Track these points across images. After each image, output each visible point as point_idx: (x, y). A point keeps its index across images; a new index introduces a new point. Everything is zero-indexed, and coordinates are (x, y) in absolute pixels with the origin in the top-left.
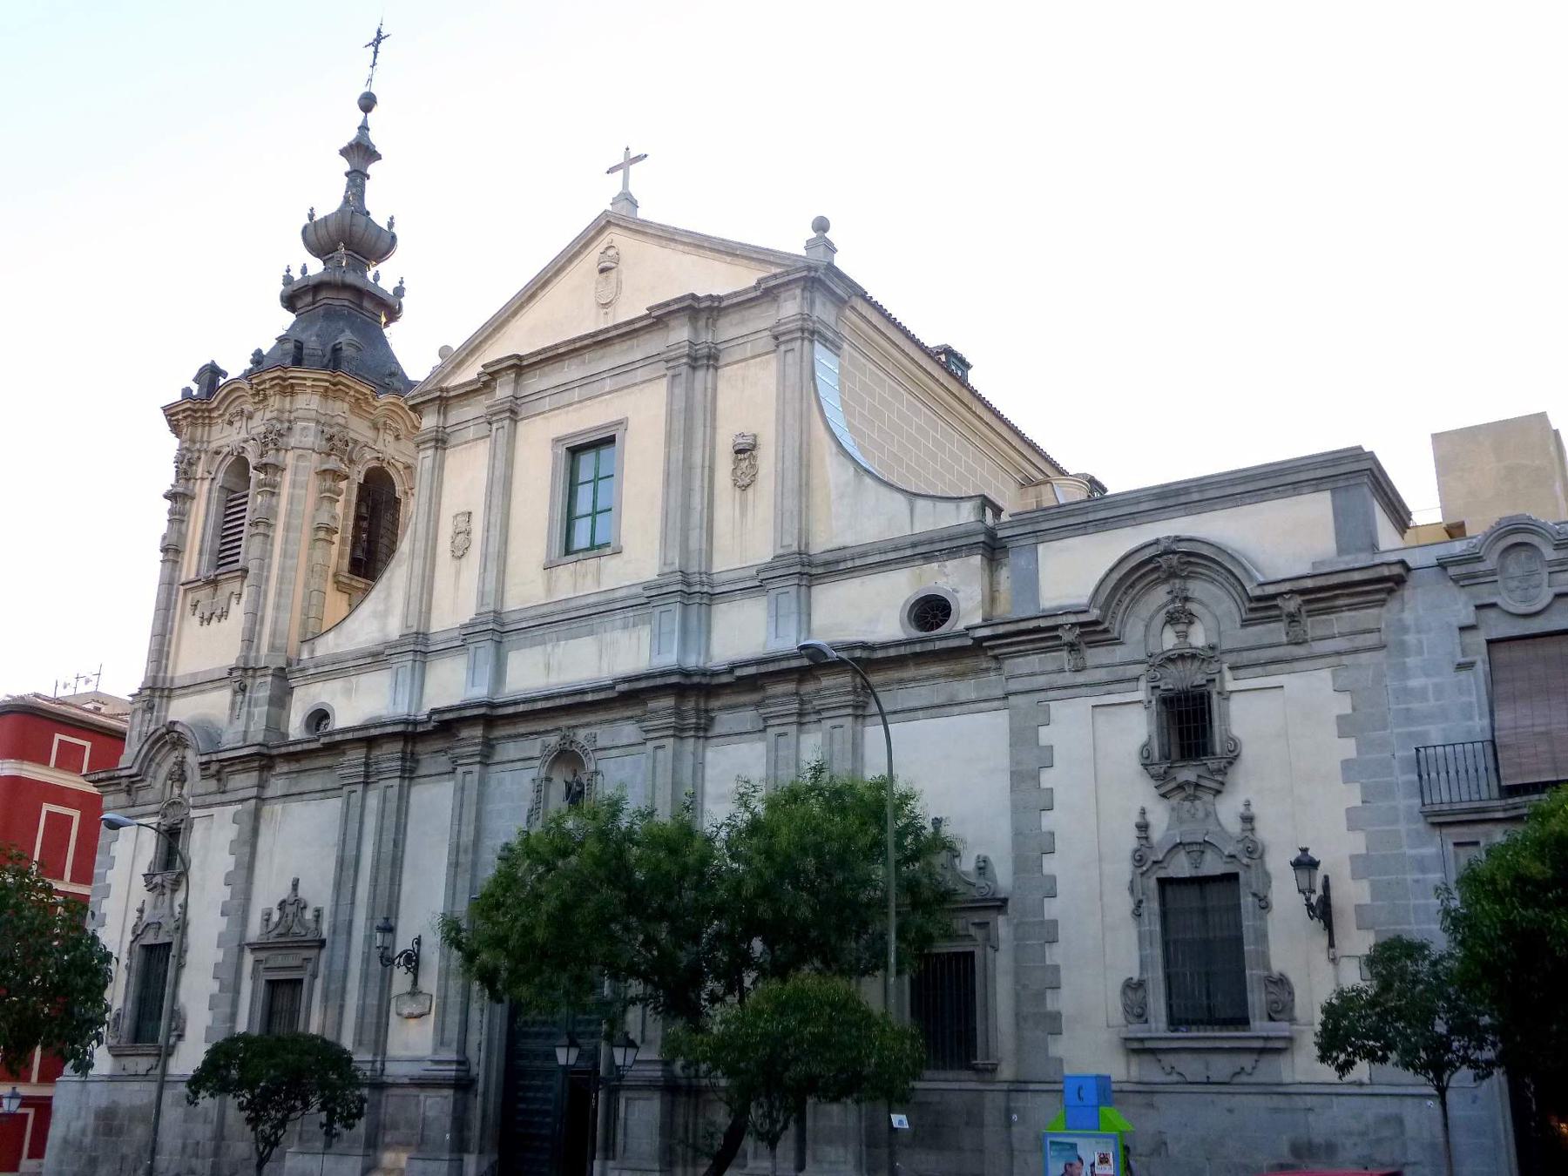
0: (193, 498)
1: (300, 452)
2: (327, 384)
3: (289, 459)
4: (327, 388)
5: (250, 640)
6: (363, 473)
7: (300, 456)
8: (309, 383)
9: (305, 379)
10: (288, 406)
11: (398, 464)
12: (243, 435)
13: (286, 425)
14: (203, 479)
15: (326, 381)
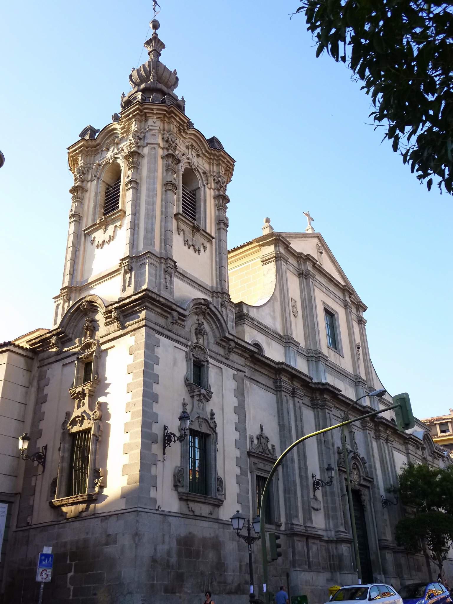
0: (87, 191)
1: (152, 146)
2: (166, 112)
3: (145, 151)
4: (165, 114)
5: (133, 244)
6: (183, 169)
7: (154, 148)
8: (155, 112)
9: (152, 109)
10: (143, 126)
11: (200, 170)
12: (116, 151)
13: (143, 135)
14: (92, 181)
15: (165, 110)
